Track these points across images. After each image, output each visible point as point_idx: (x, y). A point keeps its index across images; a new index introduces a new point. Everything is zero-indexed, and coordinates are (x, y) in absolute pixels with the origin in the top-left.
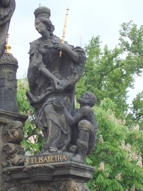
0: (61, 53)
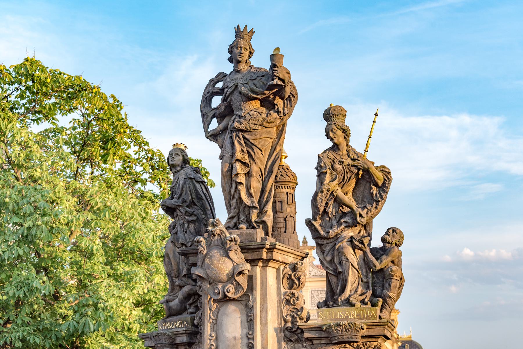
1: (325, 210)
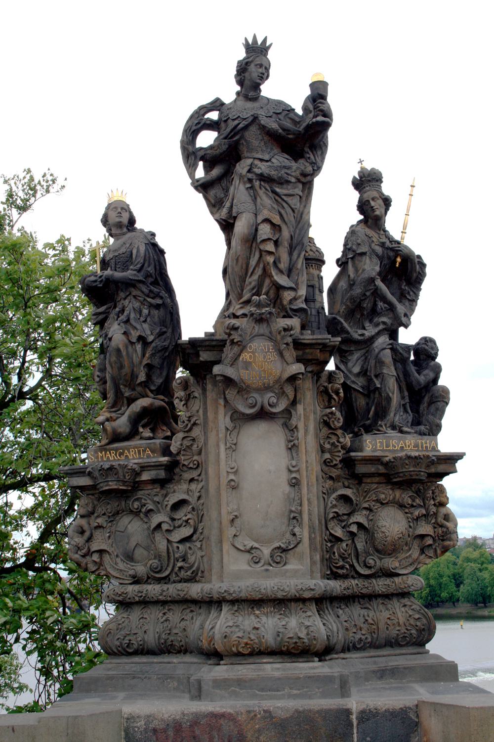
0: (399, 260)
1: (360, 303)
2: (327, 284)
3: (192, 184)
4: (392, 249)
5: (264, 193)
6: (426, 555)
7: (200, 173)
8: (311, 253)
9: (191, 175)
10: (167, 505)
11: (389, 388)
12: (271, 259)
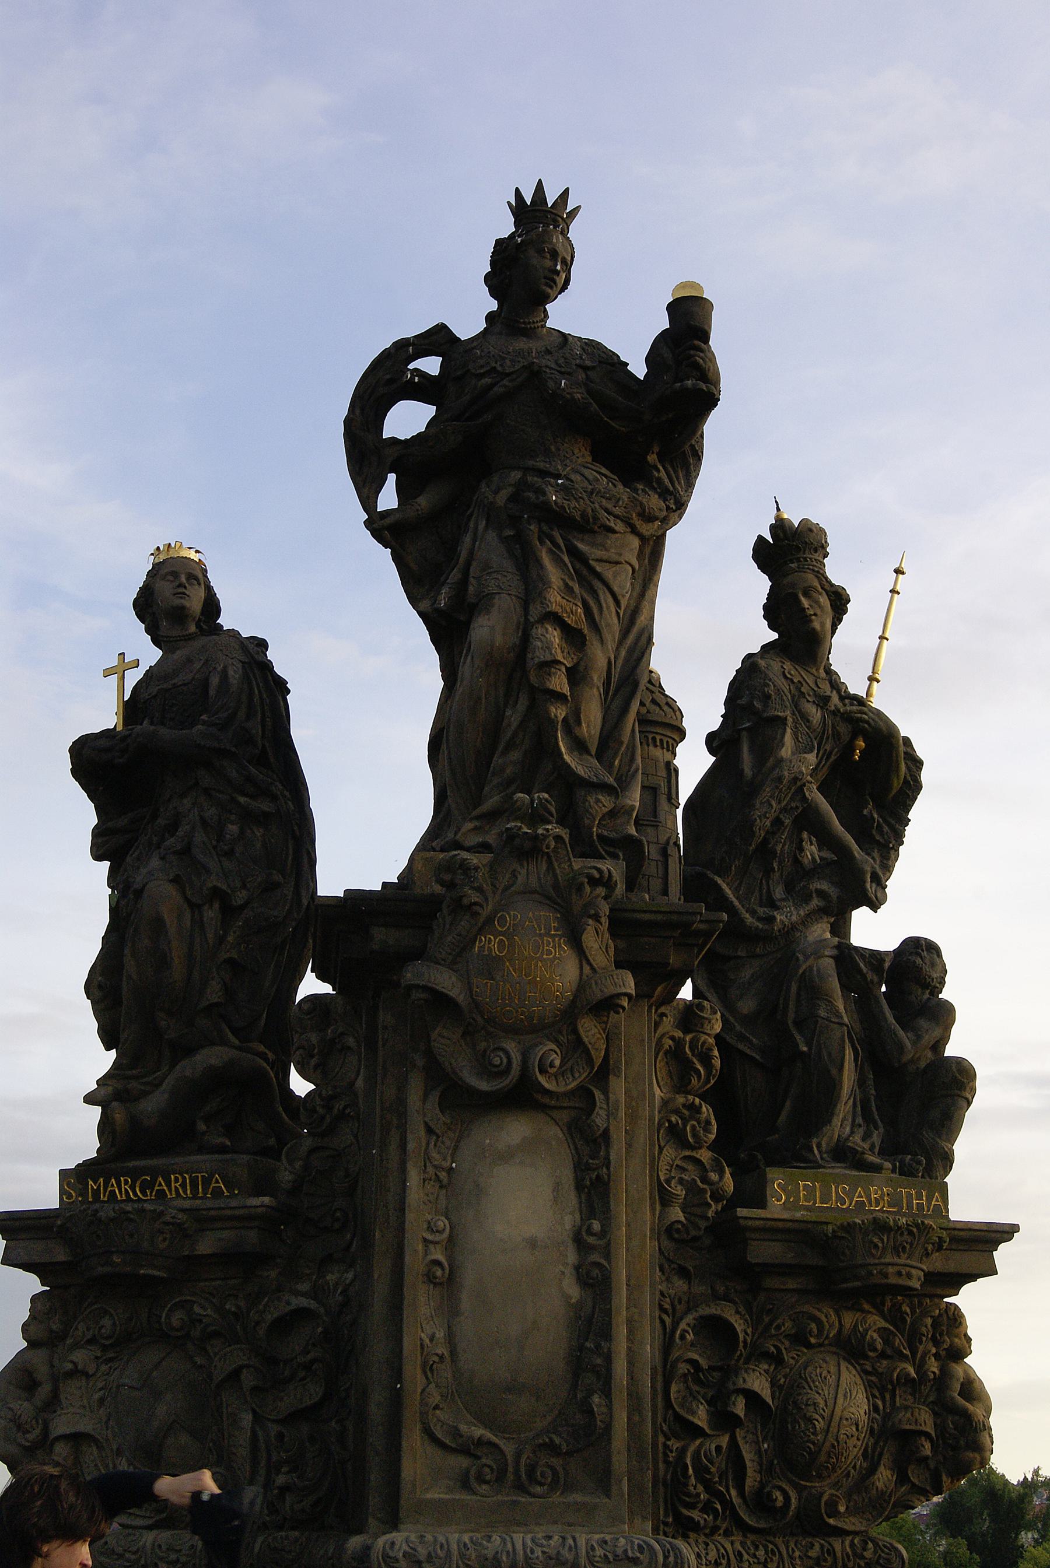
2: (686, 788)
3: (368, 524)
4: (848, 718)
5: (550, 551)
6: (913, 1484)
7: (388, 499)
8: (653, 707)
9: (368, 501)
10: (257, 1323)
11: (830, 1054)
12: (559, 712)
